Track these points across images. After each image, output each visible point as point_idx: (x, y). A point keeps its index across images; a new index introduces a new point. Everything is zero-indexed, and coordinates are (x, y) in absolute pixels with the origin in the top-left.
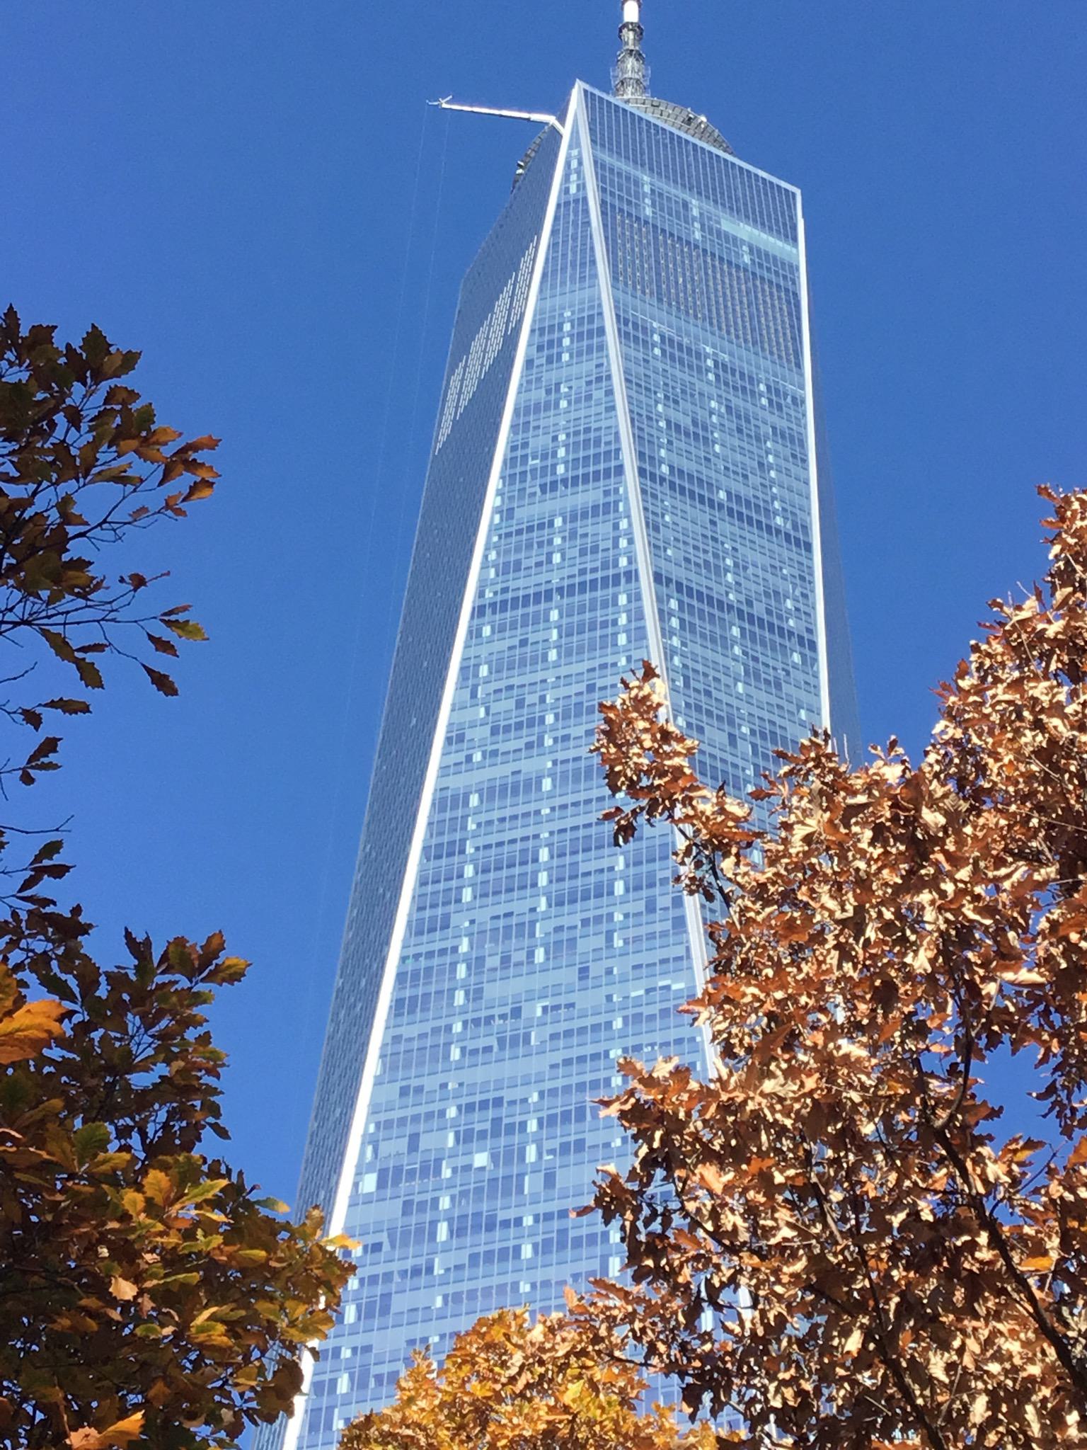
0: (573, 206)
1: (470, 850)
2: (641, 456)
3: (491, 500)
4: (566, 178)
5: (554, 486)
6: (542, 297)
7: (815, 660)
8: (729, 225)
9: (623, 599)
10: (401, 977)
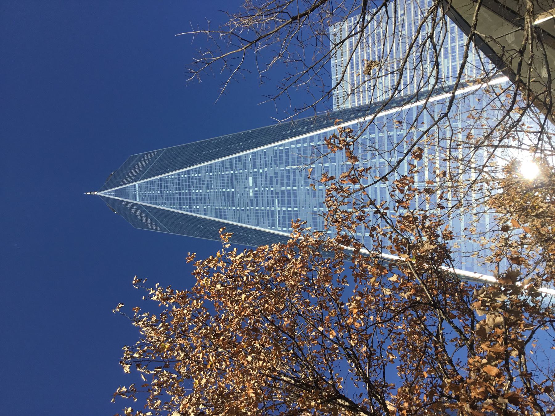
0: (116, 193)
3: (162, 207)
4: (111, 195)
5: (161, 193)
9: (182, 176)
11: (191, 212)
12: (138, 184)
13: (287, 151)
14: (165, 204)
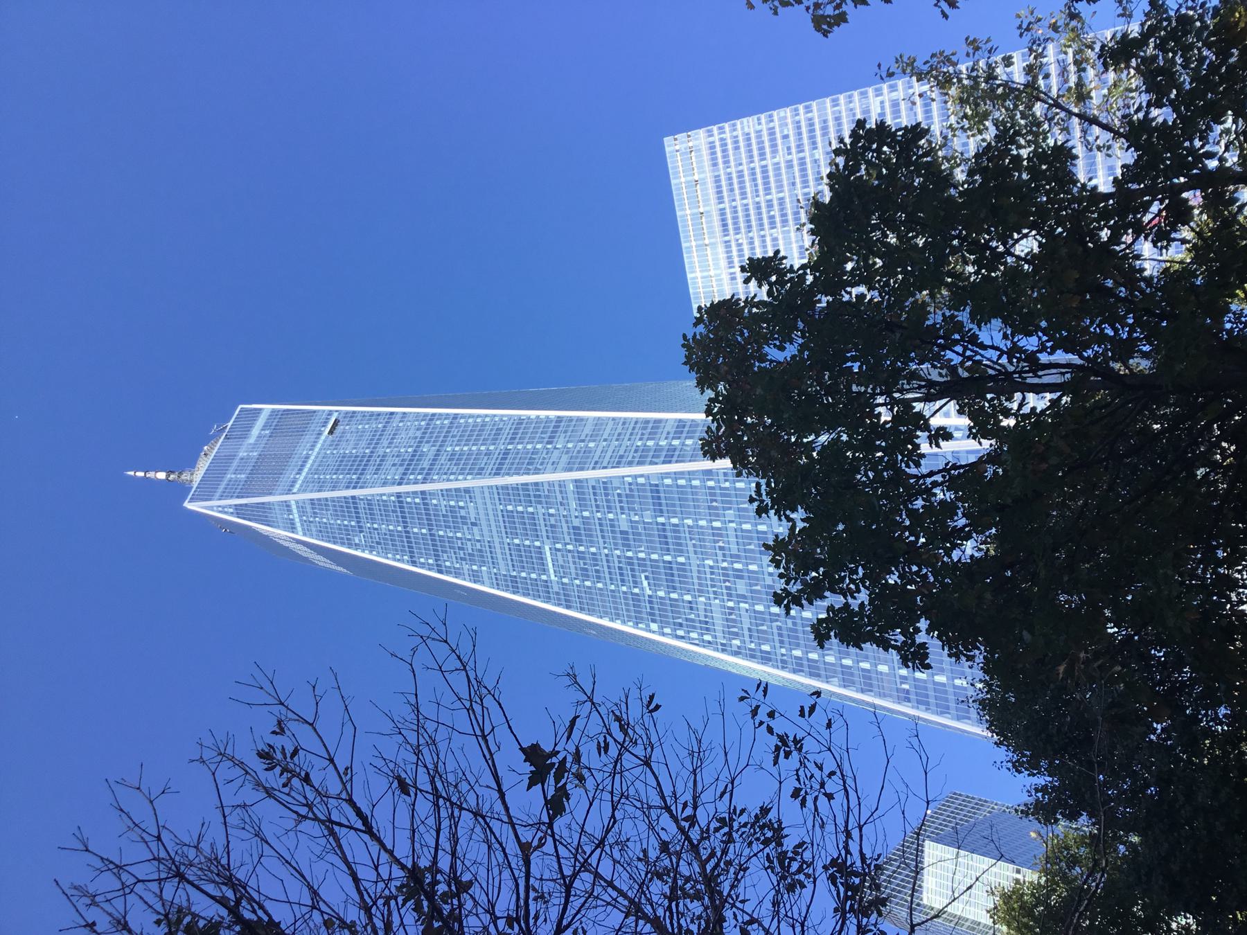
1: (514, 574)
2: (348, 487)
3: (366, 555)
4: (226, 513)
6: (278, 527)
7: (440, 414)
8: (252, 440)
9: (409, 500)
10: (568, 607)
11: (440, 572)
12: (297, 502)
13: (655, 489)
14: (371, 549)
